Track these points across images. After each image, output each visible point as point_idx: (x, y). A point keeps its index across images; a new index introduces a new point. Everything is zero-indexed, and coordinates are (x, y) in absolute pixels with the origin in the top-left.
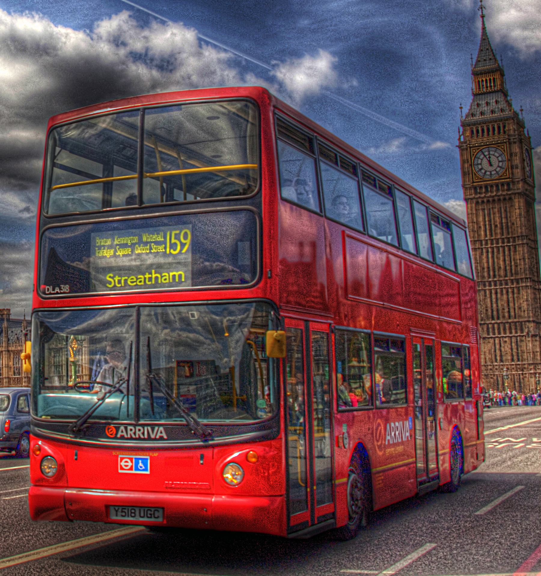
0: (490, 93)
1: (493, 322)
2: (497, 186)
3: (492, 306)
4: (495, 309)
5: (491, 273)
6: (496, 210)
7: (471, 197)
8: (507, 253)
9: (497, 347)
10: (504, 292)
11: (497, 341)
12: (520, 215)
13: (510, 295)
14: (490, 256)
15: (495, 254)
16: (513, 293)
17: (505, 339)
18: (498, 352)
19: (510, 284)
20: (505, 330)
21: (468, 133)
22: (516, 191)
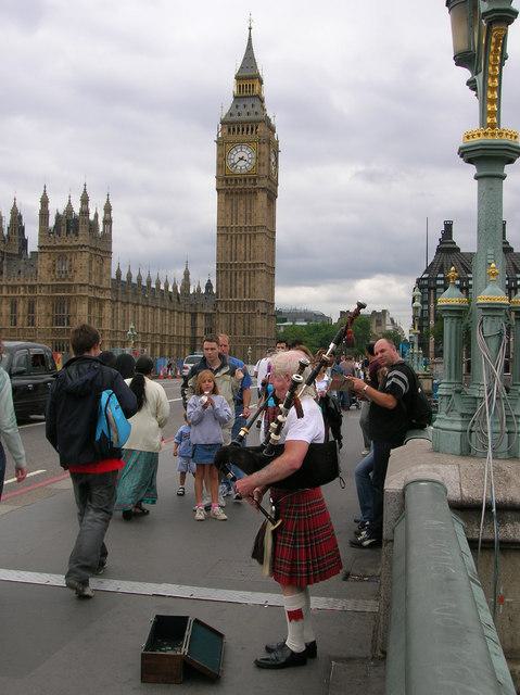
8: (248, 239)
18: (233, 326)
21: (226, 131)
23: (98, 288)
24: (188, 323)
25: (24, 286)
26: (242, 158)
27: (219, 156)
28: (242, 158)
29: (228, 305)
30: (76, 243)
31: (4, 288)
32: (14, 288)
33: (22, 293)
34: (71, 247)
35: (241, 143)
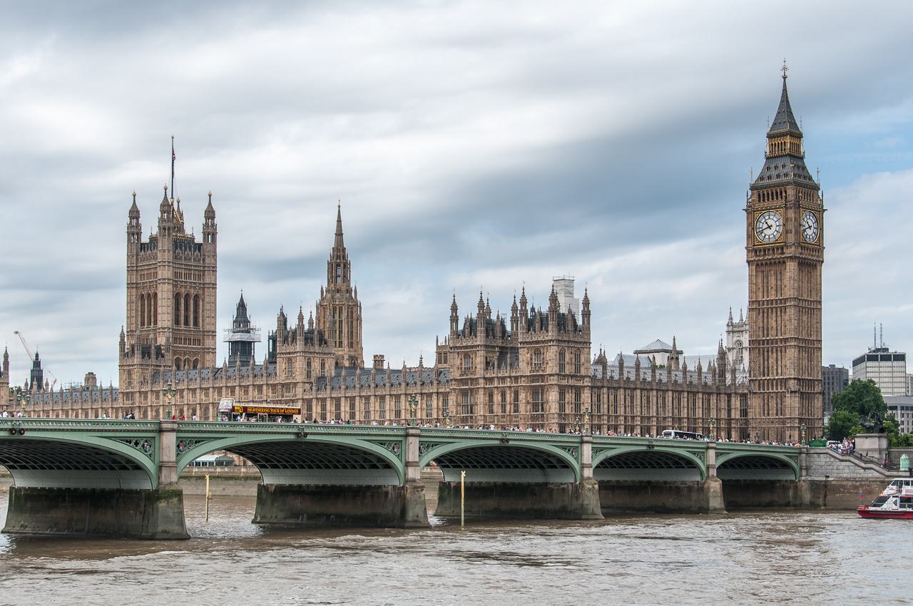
0: (780, 156)
1: (764, 378)
2: (773, 249)
3: (764, 364)
4: (766, 367)
5: (765, 332)
6: (773, 272)
7: (752, 259)
8: (779, 313)
9: (766, 402)
10: (774, 350)
11: (766, 397)
12: (790, 278)
13: (779, 354)
14: (765, 315)
15: (770, 314)
16: (781, 351)
17: (773, 395)
18: (766, 406)
19: (779, 343)
20: (772, 385)
21: (754, 198)
22: (788, 255)
23: (576, 376)
24: (723, 405)
25: (510, 377)
26: (772, 227)
27: (749, 225)
28: (772, 227)
29: (761, 384)
30: (547, 338)
31: (496, 379)
32: (503, 379)
33: (509, 385)
34: (543, 342)
35: (768, 209)
